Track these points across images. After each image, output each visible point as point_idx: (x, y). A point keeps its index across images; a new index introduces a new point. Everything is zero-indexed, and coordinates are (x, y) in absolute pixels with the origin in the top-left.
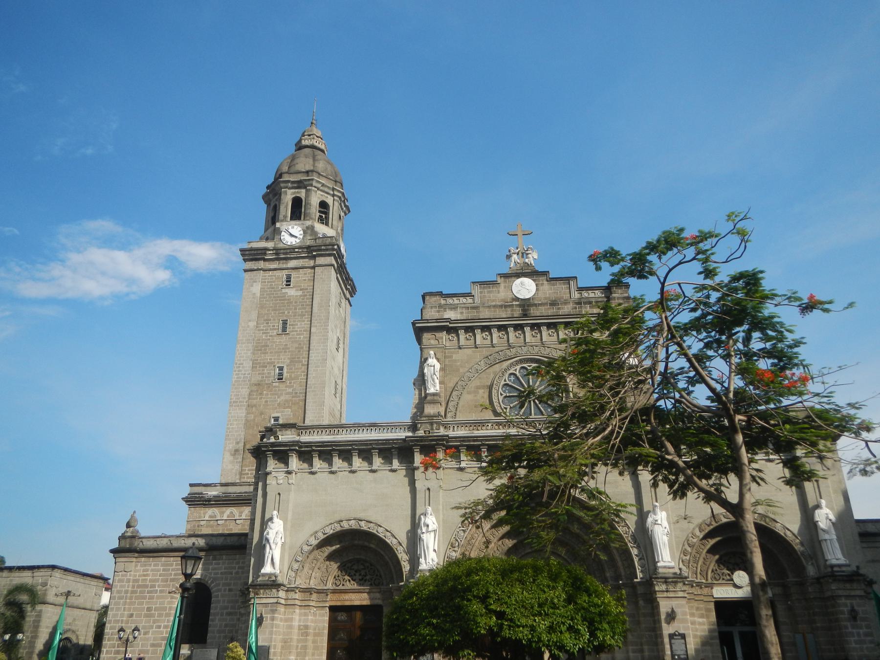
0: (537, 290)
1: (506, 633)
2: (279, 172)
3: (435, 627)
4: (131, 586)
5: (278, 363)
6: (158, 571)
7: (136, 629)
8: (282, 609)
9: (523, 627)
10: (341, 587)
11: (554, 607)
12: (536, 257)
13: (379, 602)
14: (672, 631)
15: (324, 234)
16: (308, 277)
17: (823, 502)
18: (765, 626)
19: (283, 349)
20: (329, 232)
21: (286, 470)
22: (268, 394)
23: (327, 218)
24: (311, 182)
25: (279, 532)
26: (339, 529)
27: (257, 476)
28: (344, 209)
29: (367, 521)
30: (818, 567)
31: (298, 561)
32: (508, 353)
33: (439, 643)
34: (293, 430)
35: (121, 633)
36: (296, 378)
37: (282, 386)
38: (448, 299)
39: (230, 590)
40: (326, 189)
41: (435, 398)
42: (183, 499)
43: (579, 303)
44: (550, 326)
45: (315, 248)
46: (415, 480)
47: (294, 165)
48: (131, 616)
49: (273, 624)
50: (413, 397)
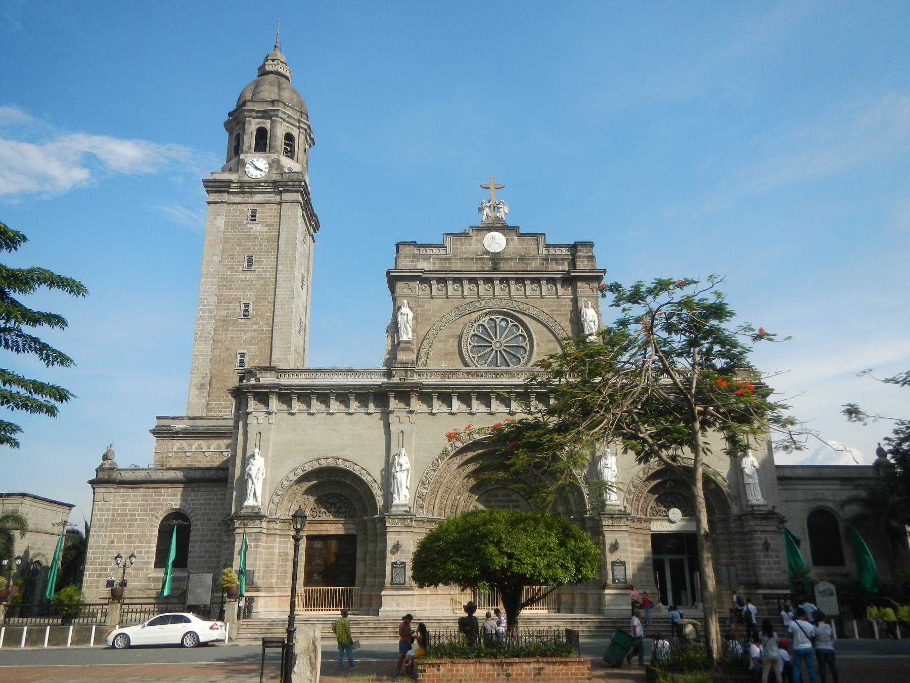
0: (507, 244)
1: (515, 569)
2: (243, 100)
3: (459, 564)
4: (111, 515)
5: (244, 299)
6: (138, 501)
7: (132, 556)
8: (264, 538)
9: (527, 564)
10: (317, 518)
11: (550, 549)
12: (507, 211)
13: (354, 532)
14: (614, 559)
15: (290, 169)
16: (274, 213)
18: (705, 565)
19: (249, 285)
20: (297, 167)
21: (266, 410)
22: (233, 330)
23: (292, 151)
24: (276, 113)
25: (261, 469)
26: (317, 466)
27: (237, 415)
28: (309, 141)
29: (344, 460)
30: (741, 506)
31: (279, 495)
32: (478, 304)
33: (463, 576)
34: (273, 372)
35: (118, 559)
36: (263, 315)
37: (248, 323)
38: (421, 249)
39: (209, 520)
40: (292, 121)
41: (408, 345)
42: (150, 431)
43: (546, 260)
44: (518, 280)
45: (281, 183)
46: (389, 423)
47: (259, 92)
48: (112, 542)
49: (257, 551)
50: (384, 344)
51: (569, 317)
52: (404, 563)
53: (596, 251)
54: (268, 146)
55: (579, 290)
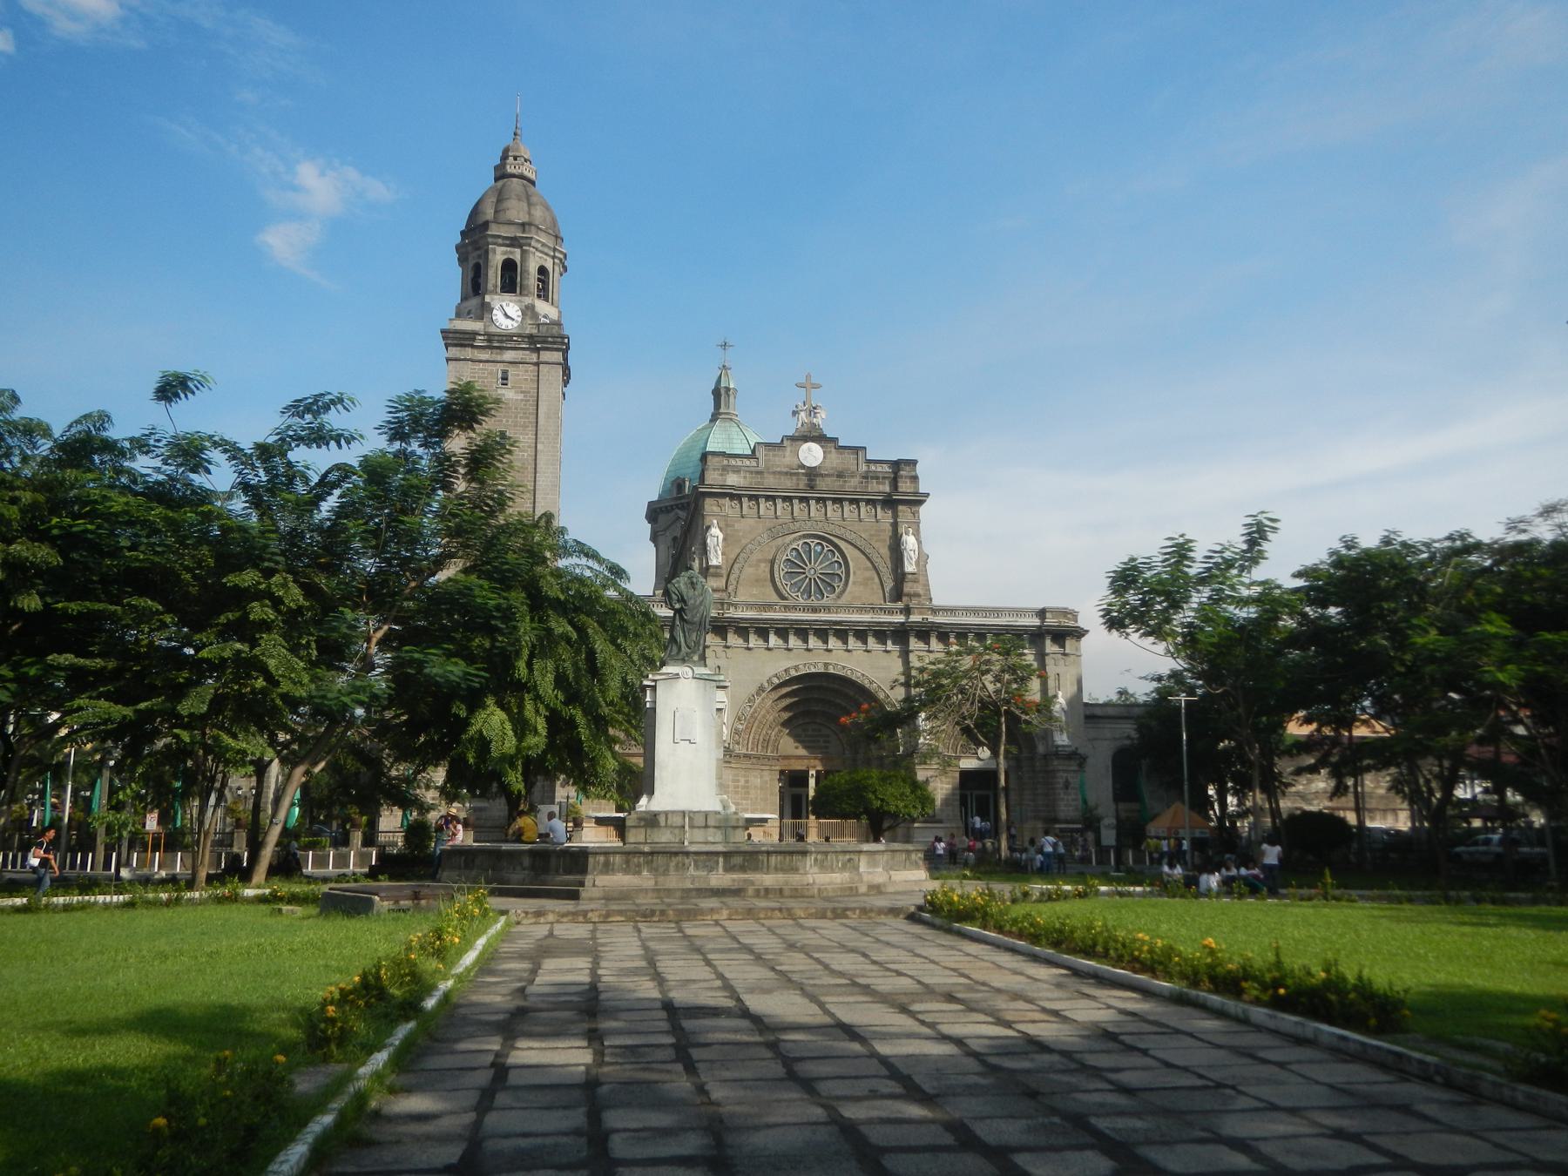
0: (824, 458)
1: (886, 808)
10: (627, 751)
17: (1060, 694)
24: (529, 241)
40: (546, 250)
41: (718, 571)
44: (835, 501)
45: (540, 339)
47: (504, 210)
53: (920, 470)
54: (519, 285)
55: (900, 514)
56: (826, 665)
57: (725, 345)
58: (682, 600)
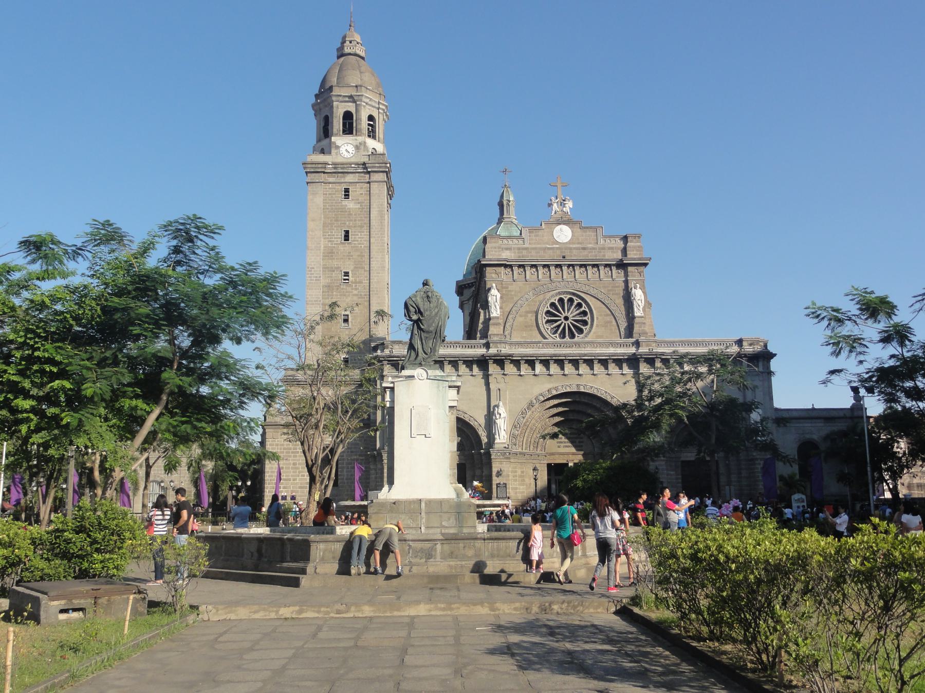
5: (344, 268)
13: (464, 462)
20: (380, 147)
24: (360, 97)
36: (360, 282)
37: (349, 289)
51: (622, 294)
52: (506, 484)
54: (354, 129)
56: (578, 385)
57: (505, 171)
58: (419, 312)
